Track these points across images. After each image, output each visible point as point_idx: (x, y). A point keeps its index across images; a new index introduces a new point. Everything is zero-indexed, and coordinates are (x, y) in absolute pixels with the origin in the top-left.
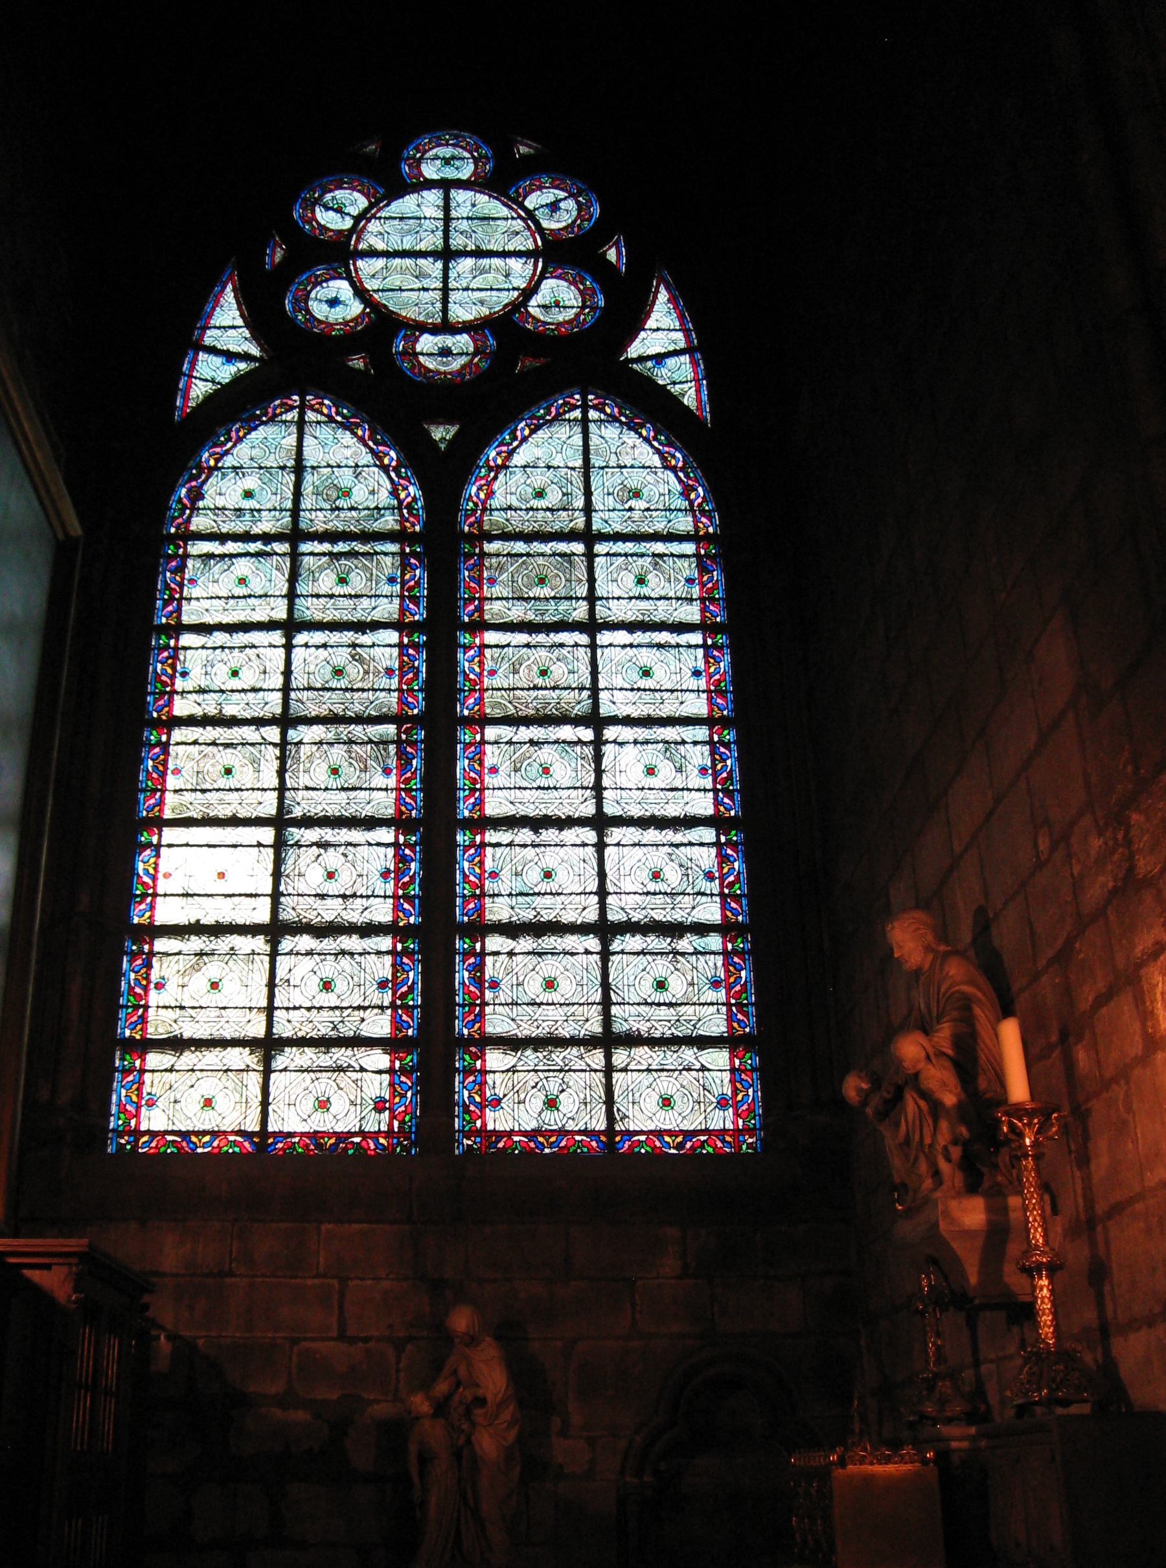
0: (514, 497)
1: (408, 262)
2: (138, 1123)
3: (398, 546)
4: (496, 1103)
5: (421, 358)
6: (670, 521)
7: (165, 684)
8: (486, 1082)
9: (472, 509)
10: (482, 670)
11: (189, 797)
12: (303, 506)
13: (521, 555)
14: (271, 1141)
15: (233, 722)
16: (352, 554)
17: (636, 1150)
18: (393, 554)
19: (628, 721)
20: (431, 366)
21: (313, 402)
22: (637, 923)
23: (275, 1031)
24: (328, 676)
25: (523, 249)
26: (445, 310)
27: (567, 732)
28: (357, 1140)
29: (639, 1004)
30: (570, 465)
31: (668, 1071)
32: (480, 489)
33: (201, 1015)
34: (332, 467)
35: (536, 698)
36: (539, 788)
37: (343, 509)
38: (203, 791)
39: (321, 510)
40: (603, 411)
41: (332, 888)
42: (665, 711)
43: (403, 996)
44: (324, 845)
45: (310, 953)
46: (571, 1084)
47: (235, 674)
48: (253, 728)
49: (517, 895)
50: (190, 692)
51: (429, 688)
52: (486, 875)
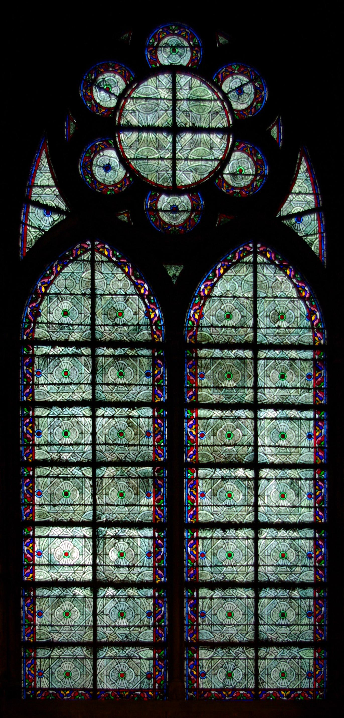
0: (214, 318)
1: (151, 135)
2: (35, 684)
3: (151, 351)
4: (204, 675)
5: (161, 214)
6: (300, 336)
7: (29, 440)
8: (199, 664)
9: (191, 327)
10: (197, 433)
11: (46, 508)
12: (97, 323)
13: (218, 358)
14: (99, 693)
15: (67, 464)
16: (125, 356)
17: (268, 698)
18: (148, 356)
19: (272, 466)
20: (166, 220)
21: (99, 246)
22: (273, 582)
23: (98, 638)
24: (116, 436)
25: (221, 126)
26: (174, 176)
27: (240, 472)
28: (139, 693)
29: (272, 625)
30: (246, 295)
31: (284, 659)
32: (195, 312)
33: (62, 630)
34: (112, 295)
35: (225, 451)
36: (226, 505)
37: (119, 325)
38: (55, 505)
39: (107, 325)
40: (265, 256)
41: (122, 562)
42: (291, 460)
43: (159, 620)
44: (117, 537)
45: (113, 597)
46: (239, 665)
47: (66, 434)
48: (77, 468)
49: (214, 566)
50: (43, 445)
51: (169, 444)
52: (199, 555)
